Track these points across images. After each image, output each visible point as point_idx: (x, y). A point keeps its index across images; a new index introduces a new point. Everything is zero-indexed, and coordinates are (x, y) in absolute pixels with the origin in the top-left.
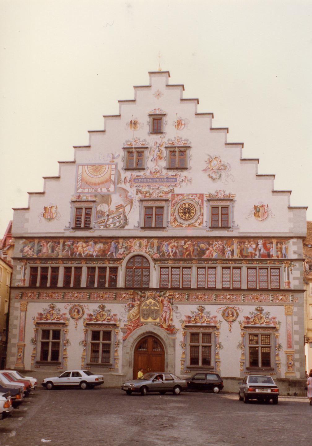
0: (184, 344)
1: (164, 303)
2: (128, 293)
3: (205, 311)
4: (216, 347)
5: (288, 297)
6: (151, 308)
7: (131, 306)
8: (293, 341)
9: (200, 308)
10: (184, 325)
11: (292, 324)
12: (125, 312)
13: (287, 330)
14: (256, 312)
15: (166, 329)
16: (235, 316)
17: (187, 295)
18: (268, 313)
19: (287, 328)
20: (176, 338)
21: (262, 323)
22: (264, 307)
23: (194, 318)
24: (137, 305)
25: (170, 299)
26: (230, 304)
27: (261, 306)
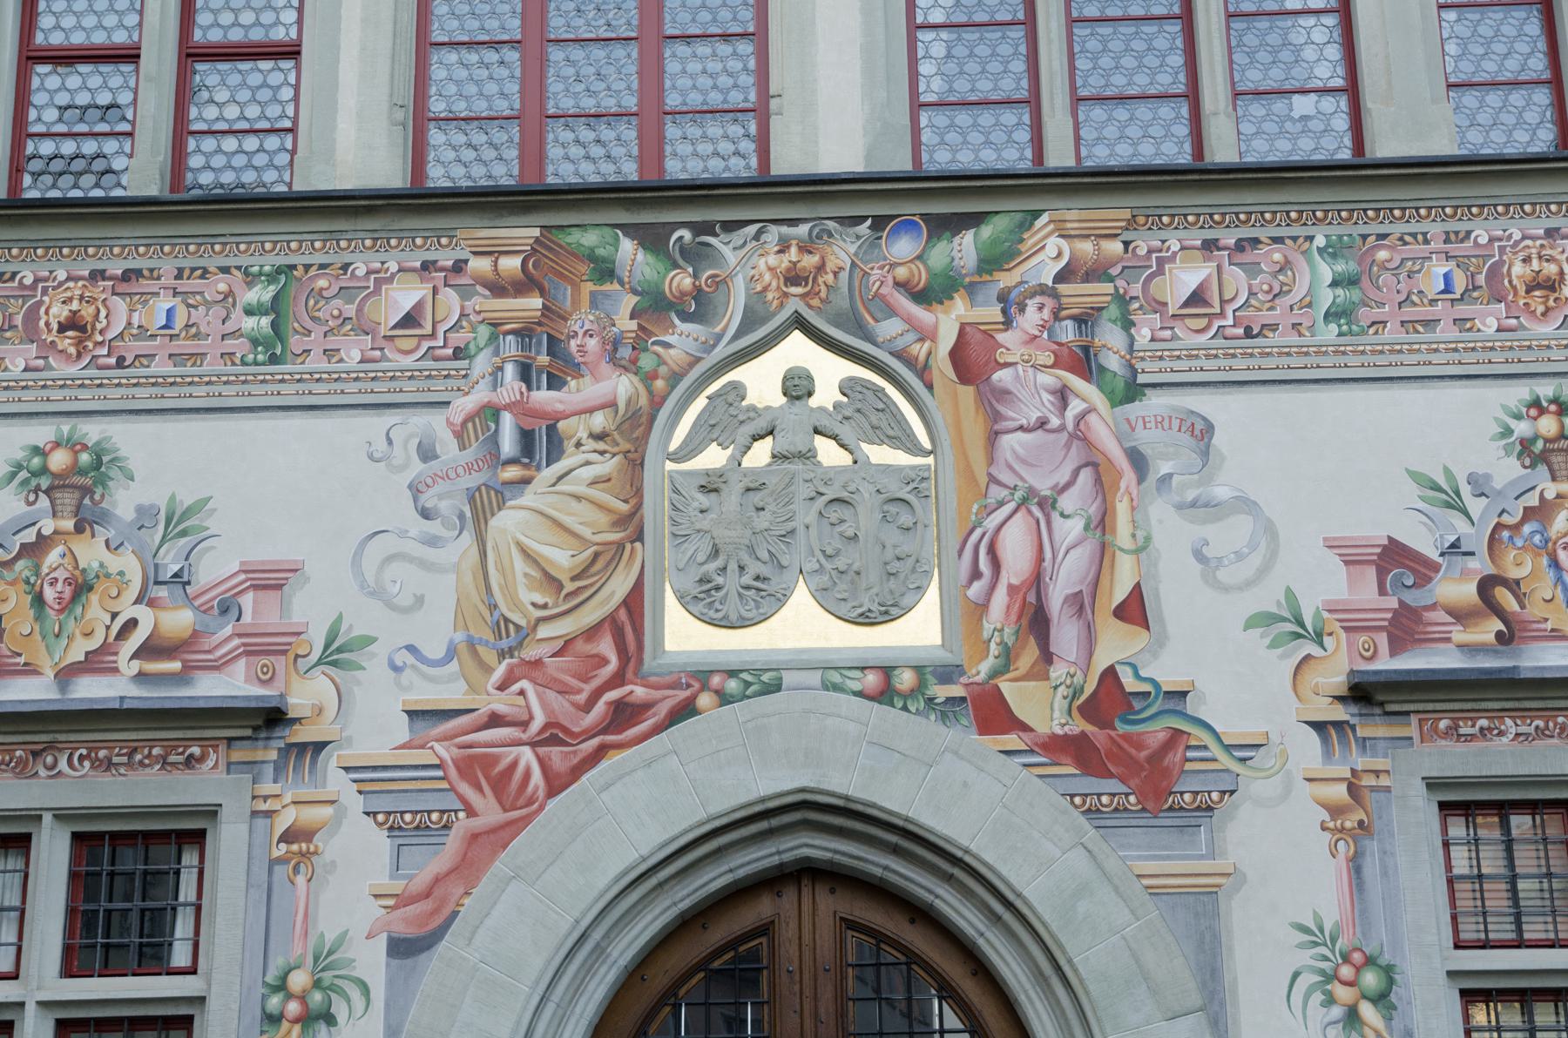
0: (1370, 961)
1: (1001, 377)
2: (459, 267)
6: (809, 455)
7: (508, 444)
9: (1548, 425)
10: (1334, 675)
12: (418, 526)
15: (1057, 746)
17: (1332, 251)
23: (1480, 565)
24: (599, 421)
25: (1081, 321)
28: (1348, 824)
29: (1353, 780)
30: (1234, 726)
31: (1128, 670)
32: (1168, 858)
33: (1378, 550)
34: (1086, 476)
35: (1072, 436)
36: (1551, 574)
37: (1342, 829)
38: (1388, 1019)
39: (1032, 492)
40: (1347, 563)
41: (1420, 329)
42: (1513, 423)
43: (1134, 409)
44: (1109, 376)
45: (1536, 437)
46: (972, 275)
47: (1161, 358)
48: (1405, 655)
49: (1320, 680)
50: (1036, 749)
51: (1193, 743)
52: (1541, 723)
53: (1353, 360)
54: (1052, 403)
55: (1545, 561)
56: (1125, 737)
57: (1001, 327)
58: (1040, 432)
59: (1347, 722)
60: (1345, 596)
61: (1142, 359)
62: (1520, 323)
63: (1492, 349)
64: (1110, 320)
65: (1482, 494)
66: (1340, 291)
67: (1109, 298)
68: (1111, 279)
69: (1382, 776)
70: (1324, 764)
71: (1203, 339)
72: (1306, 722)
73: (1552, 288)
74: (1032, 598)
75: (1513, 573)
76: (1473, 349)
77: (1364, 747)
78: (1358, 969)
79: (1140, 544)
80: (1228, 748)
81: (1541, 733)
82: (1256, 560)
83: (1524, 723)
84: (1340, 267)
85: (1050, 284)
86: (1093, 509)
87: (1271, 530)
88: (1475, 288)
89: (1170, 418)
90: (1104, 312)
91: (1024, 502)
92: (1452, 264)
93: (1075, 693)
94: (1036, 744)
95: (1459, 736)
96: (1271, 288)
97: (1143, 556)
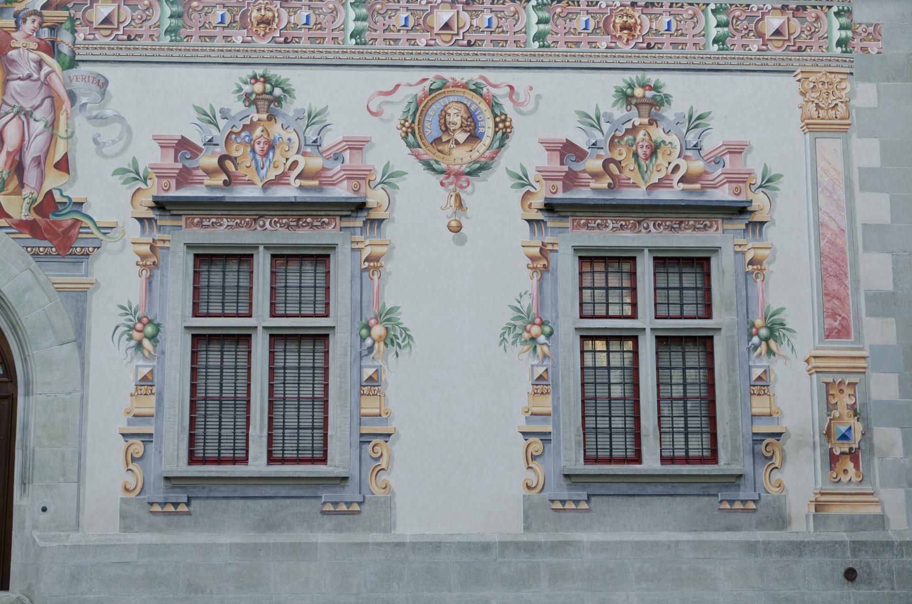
0: (150, 322)
1: (12, 54)
3: (290, 108)
4: (363, 339)
5: (818, 18)
8: (856, 290)
9: (258, 87)
11: (849, 186)
13: (819, 224)
14: (619, 113)
15: (22, 225)
16: (486, 140)
18: (696, 121)
19: (817, 209)
20: (95, 284)
21: (660, 184)
22: (671, 83)
23: (220, 150)
25: (54, 29)
26: (456, 60)
27: (652, 78)
28: (148, 263)
29: (153, 244)
30: (102, 218)
31: (58, 192)
32: (67, 276)
33: (176, 142)
34: (47, 102)
35: (43, 83)
36: (251, 155)
37: (145, 265)
38: (155, 346)
39: (22, 108)
40: (162, 147)
41: (208, 40)
42: (243, 86)
43: (73, 72)
44: (62, 56)
45: (253, 92)
46: (3, 4)
47: (87, 48)
48: (183, 189)
49: (143, 199)
50: (13, 226)
51: (83, 225)
52: (238, 221)
53: (175, 53)
54: (35, 67)
55: (249, 149)
56: (54, 222)
57: (14, 29)
58: (28, 81)
59: (153, 218)
60: (159, 162)
61: (79, 48)
62: (252, 39)
63: (238, 51)
64: (65, 29)
65: (226, 118)
66: (173, 20)
67: (66, 18)
68: (68, 9)
69: (166, 242)
70: (141, 237)
71: (108, 40)
72: (135, 218)
73: (269, 24)
74: (17, 158)
75: (234, 154)
76: (230, 51)
77: (160, 230)
78: (144, 325)
79: (69, 135)
80: (99, 228)
81: (238, 225)
82: (121, 144)
83: (231, 221)
84: (175, 9)
85: (39, 10)
86: (49, 118)
87: (129, 130)
88: (235, 22)
89: (89, 77)
90: (63, 25)
91: (18, 113)
92: (226, 10)
93: (33, 202)
94: (13, 224)
95: (203, 225)
96: (142, 18)
97: (70, 140)
